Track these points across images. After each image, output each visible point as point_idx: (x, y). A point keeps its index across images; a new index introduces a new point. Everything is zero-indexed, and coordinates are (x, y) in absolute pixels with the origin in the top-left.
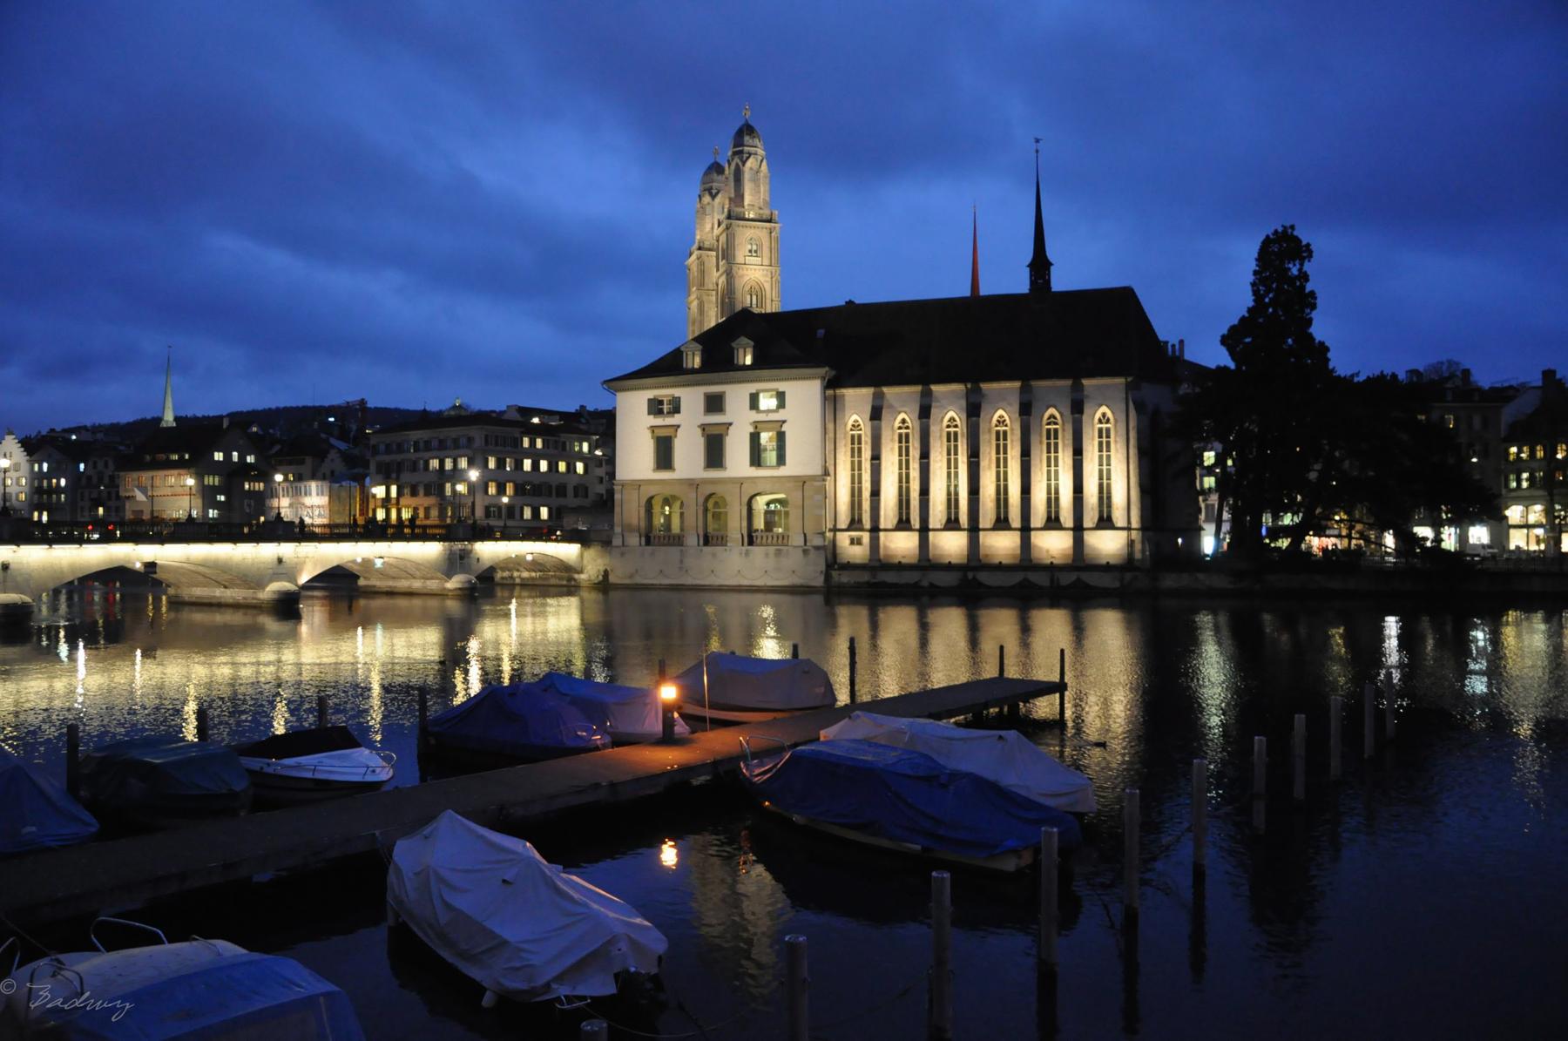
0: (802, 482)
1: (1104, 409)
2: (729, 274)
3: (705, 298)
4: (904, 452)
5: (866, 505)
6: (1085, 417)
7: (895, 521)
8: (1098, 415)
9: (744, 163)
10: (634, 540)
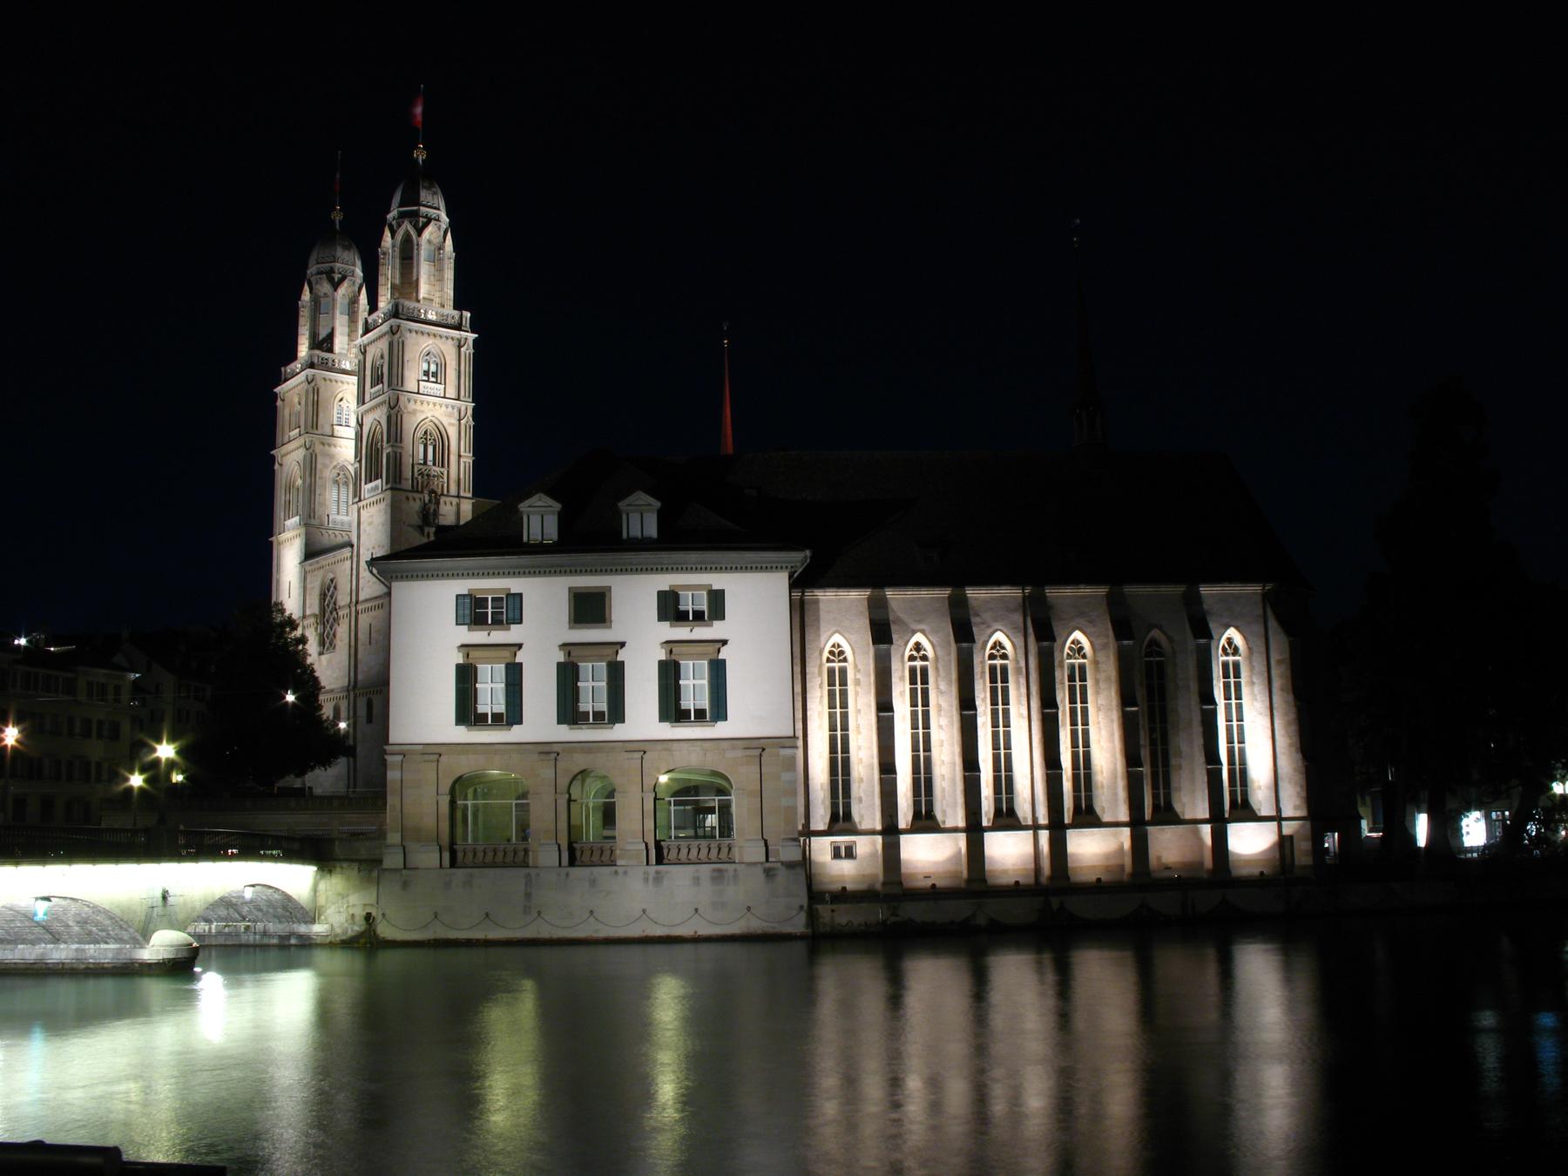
0: (758, 747)
3: (318, 448)
9: (420, 234)
10: (428, 857)
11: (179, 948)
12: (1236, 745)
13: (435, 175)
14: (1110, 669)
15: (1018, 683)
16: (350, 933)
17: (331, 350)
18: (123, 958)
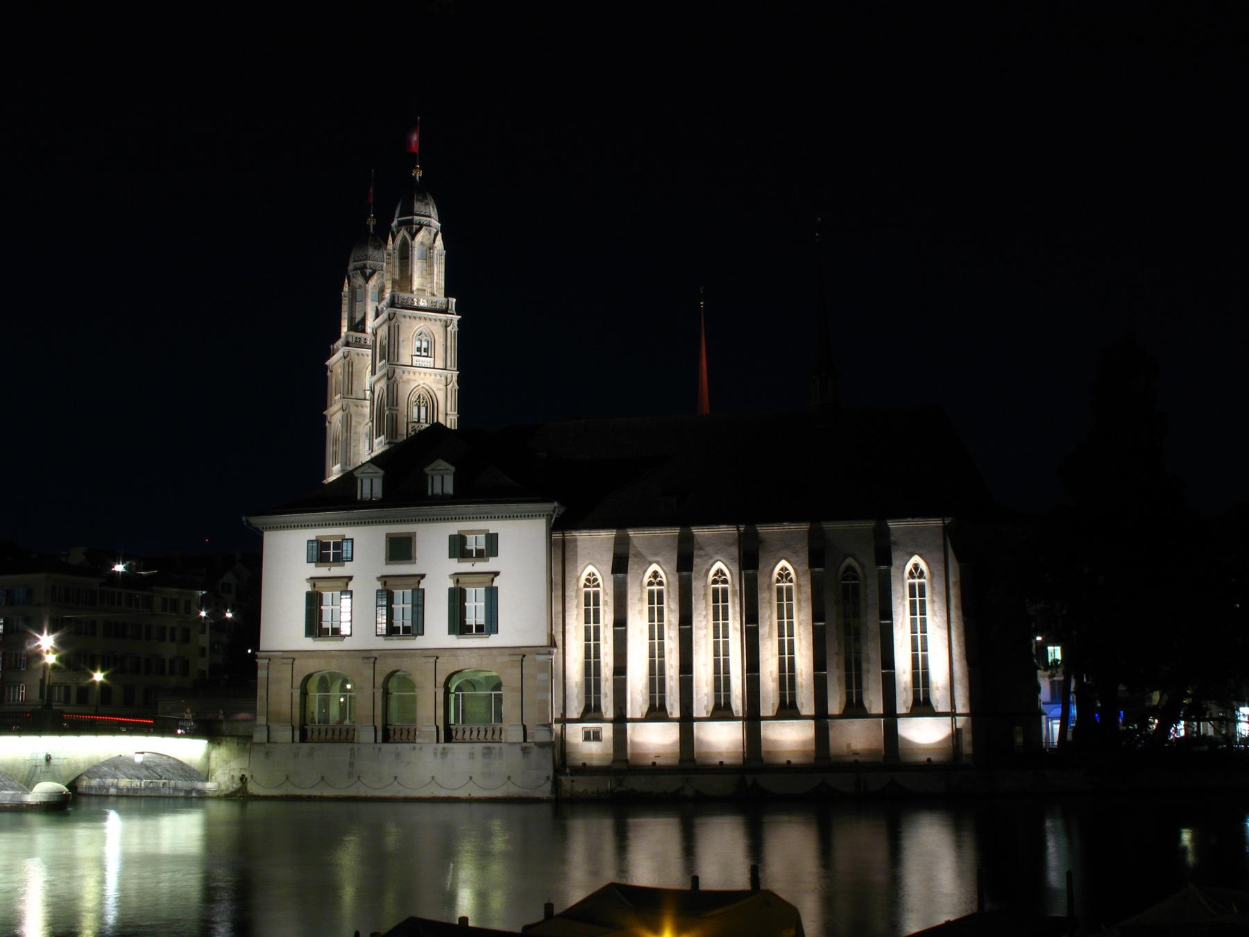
0: (520, 654)
1: (916, 559)
2: (391, 378)
3: (353, 409)
4: (656, 614)
5: (607, 687)
6: (894, 571)
7: (645, 709)
8: (909, 567)
9: (413, 237)
10: (284, 734)
11: (51, 794)
12: (920, 653)
13: (427, 189)
14: (807, 590)
15: (733, 602)
16: (231, 789)
17: (364, 331)
18: (16, 801)
